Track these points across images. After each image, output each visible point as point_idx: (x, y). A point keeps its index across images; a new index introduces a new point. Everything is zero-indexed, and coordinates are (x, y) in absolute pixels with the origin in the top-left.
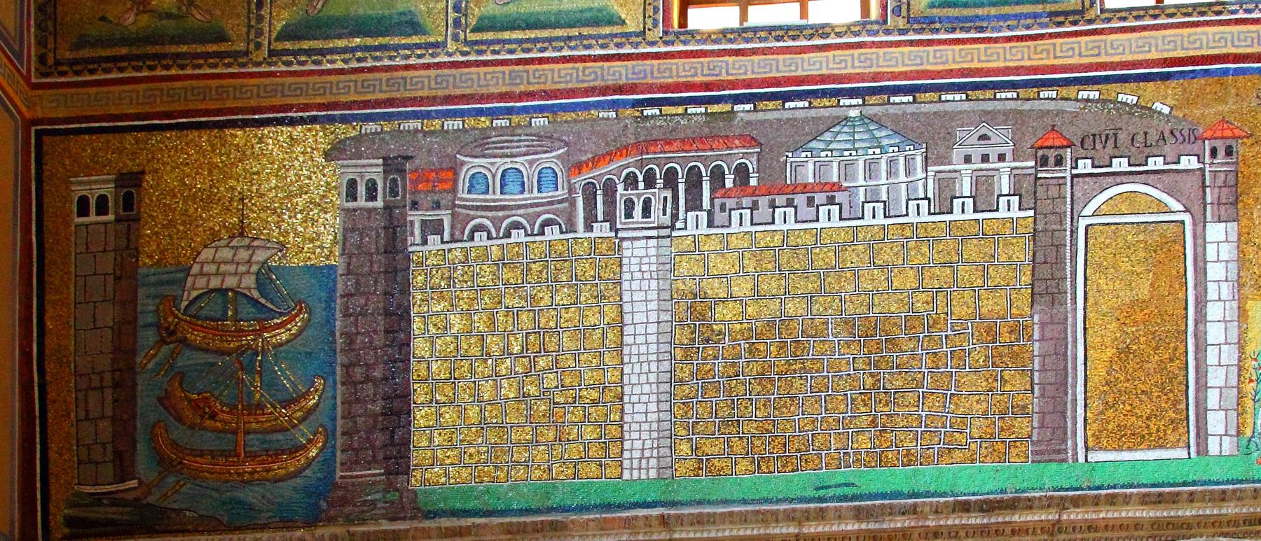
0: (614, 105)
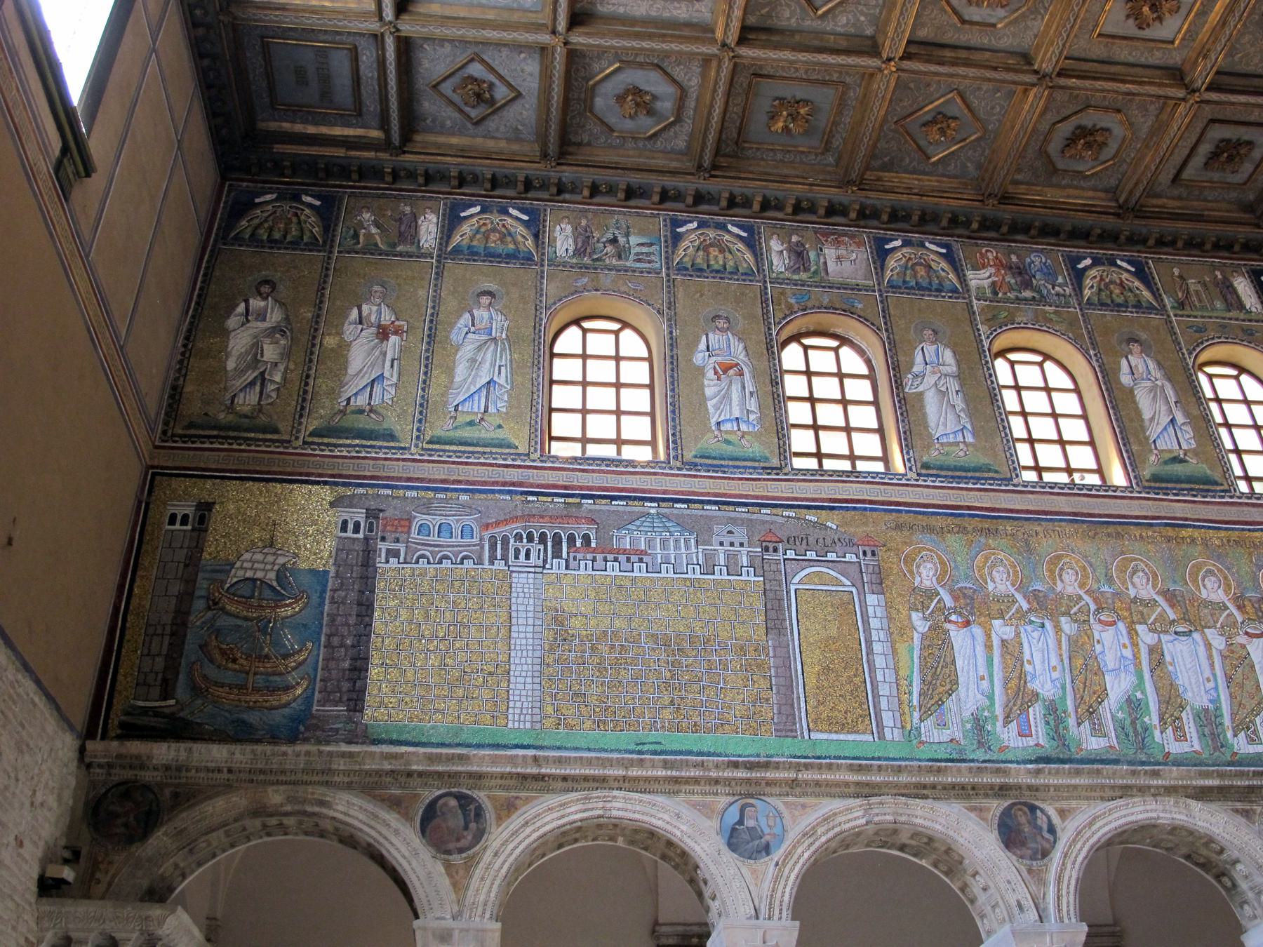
0: (509, 492)
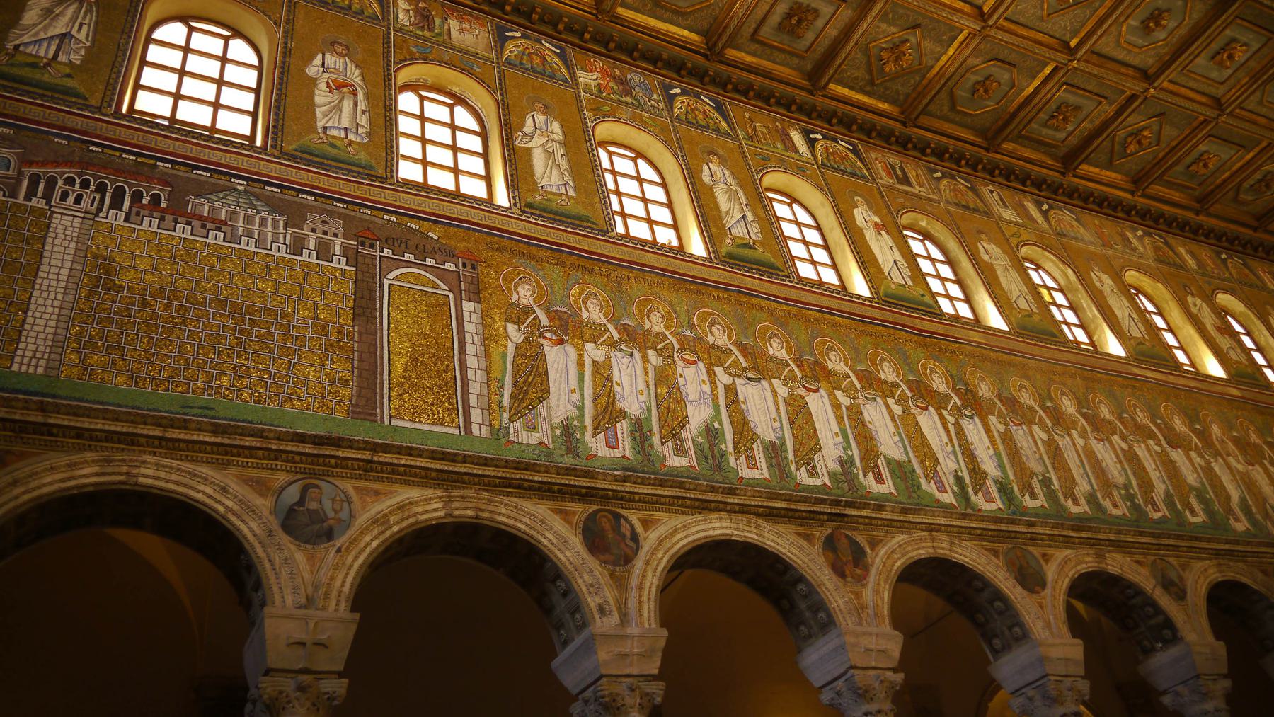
0: (67, 138)
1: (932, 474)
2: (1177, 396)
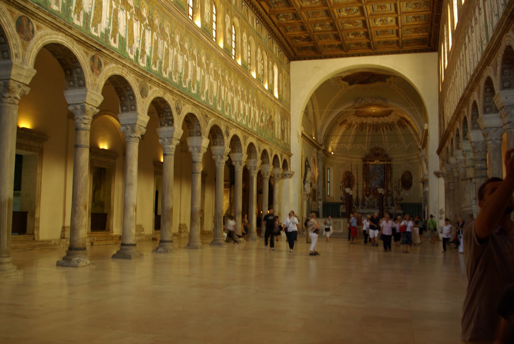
1: (131, 47)
2: (208, 49)
